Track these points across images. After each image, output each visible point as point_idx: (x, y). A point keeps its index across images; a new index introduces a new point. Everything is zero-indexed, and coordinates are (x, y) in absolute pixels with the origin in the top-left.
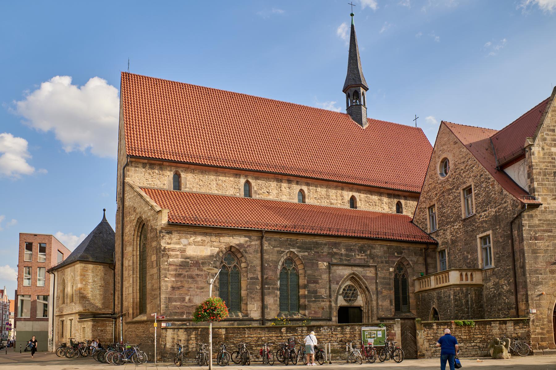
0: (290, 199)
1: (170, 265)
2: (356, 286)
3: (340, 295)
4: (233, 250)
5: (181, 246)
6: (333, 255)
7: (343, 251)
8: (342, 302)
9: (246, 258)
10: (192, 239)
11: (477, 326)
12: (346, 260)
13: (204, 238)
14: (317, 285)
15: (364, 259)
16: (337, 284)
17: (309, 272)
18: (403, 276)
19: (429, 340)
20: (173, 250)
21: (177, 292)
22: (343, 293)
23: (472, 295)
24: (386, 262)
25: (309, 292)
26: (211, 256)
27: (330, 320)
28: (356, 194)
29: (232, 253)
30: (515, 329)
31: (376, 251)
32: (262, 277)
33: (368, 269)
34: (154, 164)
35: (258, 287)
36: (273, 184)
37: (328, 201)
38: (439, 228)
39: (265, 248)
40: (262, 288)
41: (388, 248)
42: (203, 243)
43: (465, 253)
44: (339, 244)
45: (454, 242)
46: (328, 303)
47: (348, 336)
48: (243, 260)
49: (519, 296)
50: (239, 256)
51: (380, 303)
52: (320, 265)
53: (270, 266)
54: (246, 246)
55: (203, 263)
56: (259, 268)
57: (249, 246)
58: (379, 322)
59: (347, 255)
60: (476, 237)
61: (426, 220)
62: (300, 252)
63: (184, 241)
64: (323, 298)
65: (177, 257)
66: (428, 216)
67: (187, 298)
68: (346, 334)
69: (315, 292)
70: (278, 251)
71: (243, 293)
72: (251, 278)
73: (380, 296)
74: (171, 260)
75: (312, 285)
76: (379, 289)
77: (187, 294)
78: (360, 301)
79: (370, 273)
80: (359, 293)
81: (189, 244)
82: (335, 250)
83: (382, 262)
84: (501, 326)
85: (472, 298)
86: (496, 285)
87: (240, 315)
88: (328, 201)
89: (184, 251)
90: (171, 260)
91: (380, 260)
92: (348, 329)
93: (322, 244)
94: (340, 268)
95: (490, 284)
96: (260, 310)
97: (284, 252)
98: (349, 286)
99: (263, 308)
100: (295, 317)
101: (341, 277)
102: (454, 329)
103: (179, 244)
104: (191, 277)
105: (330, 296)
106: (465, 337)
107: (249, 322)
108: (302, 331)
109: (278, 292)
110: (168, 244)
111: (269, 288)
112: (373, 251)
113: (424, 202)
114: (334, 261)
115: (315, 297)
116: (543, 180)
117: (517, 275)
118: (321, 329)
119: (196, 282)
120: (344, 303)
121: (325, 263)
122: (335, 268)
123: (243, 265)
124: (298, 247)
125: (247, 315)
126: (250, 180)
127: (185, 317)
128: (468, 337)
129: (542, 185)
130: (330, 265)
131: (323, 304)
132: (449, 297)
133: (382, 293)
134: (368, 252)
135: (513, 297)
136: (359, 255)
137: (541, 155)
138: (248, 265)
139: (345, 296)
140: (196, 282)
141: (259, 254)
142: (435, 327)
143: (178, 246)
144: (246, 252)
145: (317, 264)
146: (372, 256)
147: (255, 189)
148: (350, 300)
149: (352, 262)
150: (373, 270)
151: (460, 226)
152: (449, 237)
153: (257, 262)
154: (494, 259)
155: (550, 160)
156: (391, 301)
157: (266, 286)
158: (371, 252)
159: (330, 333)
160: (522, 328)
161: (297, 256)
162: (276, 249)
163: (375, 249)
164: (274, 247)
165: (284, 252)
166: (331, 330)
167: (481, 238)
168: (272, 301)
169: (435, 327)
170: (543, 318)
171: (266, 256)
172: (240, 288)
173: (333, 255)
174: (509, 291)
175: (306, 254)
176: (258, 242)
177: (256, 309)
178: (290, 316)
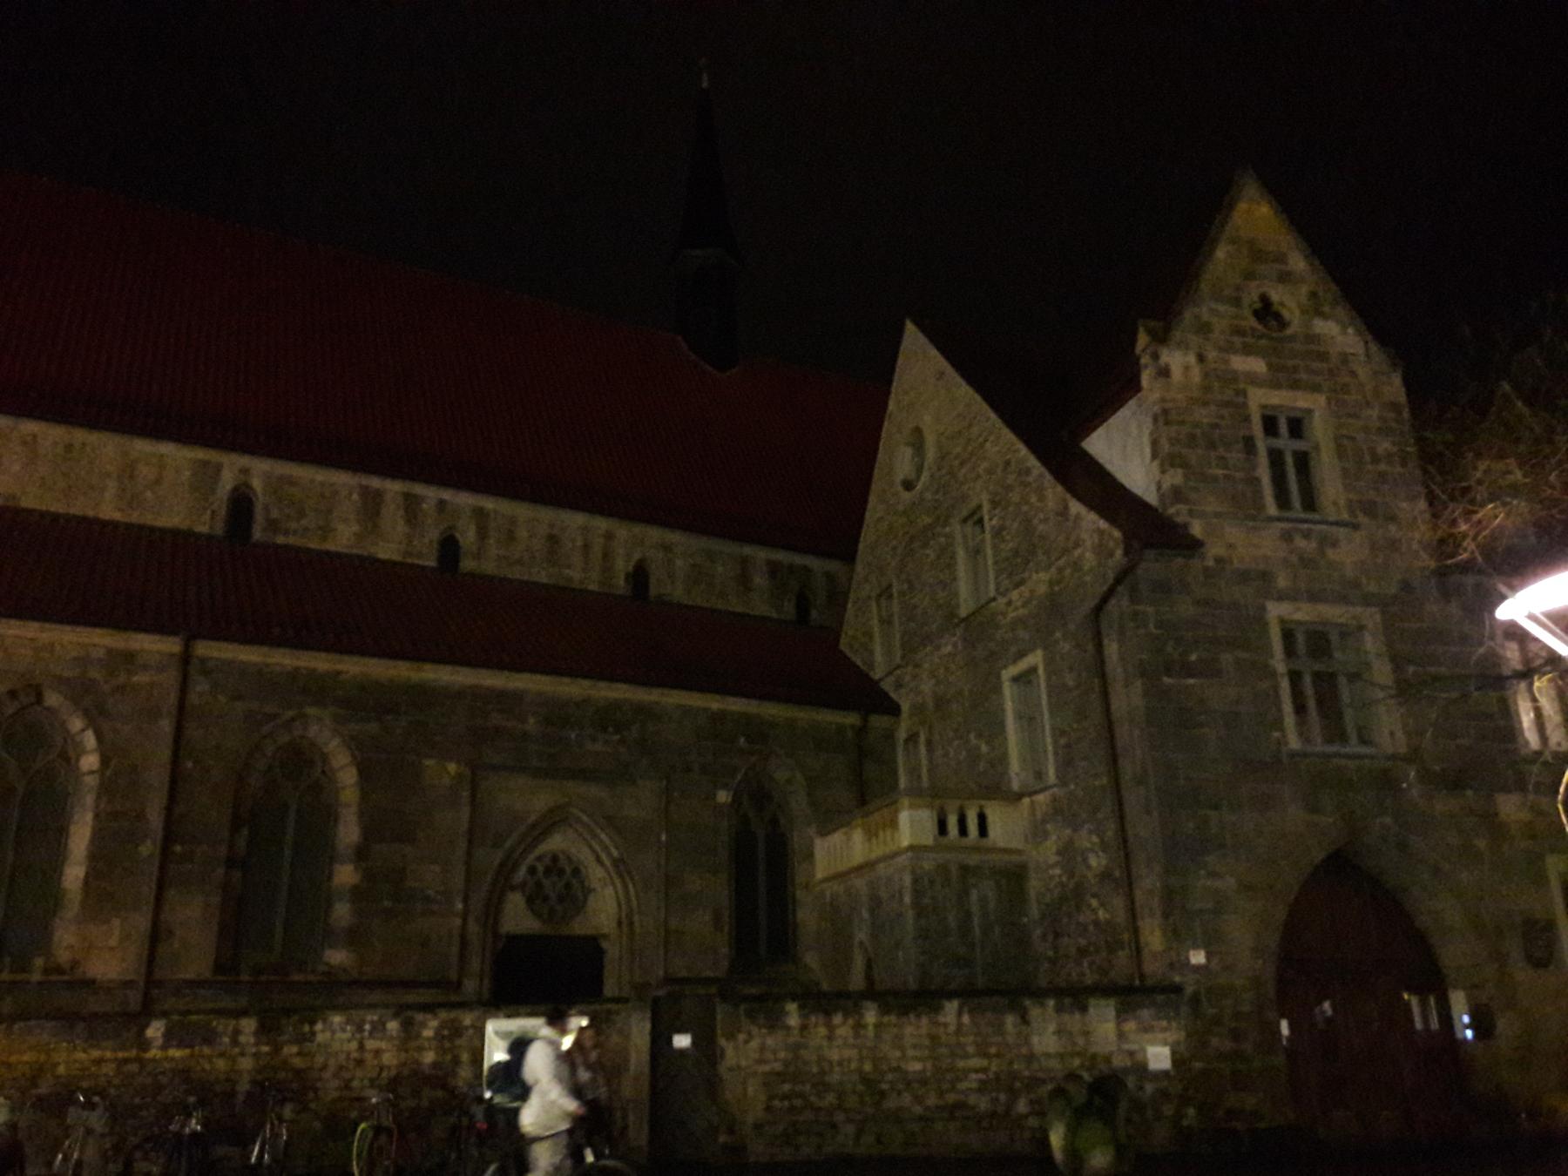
11: (966, 1019)
18: (774, 822)
23: (983, 894)
30: (1121, 1035)
38: (903, 657)
39: (193, 698)
43: (972, 736)
45: (941, 702)
49: (1138, 894)
54: (106, 688)
57: (121, 689)
60: (999, 677)
61: (871, 637)
64: (427, 899)
66: (875, 622)
68: (420, 1049)
71: (74, 874)
84: (1066, 1017)
85: (983, 900)
86: (1067, 852)
92: (430, 1028)
95: (1048, 851)
97: (275, 716)
98: (555, 859)
99: (157, 935)
102: (871, 1032)
106: (917, 1066)
113: (866, 580)
117: (1127, 809)
118: (319, 1026)
121: (452, 767)
128: (929, 1065)
132: (901, 900)
135: (1119, 903)
138: (105, 761)
142: (793, 1020)
147: (275, 514)
151: (955, 645)
152: (927, 687)
154: (1056, 754)
157: (178, 848)
159: (354, 1045)
166: (360, 1029)
167: (1015, 679)
169: (793, 1020)
174: (1105, 876)
177: (113, 942)
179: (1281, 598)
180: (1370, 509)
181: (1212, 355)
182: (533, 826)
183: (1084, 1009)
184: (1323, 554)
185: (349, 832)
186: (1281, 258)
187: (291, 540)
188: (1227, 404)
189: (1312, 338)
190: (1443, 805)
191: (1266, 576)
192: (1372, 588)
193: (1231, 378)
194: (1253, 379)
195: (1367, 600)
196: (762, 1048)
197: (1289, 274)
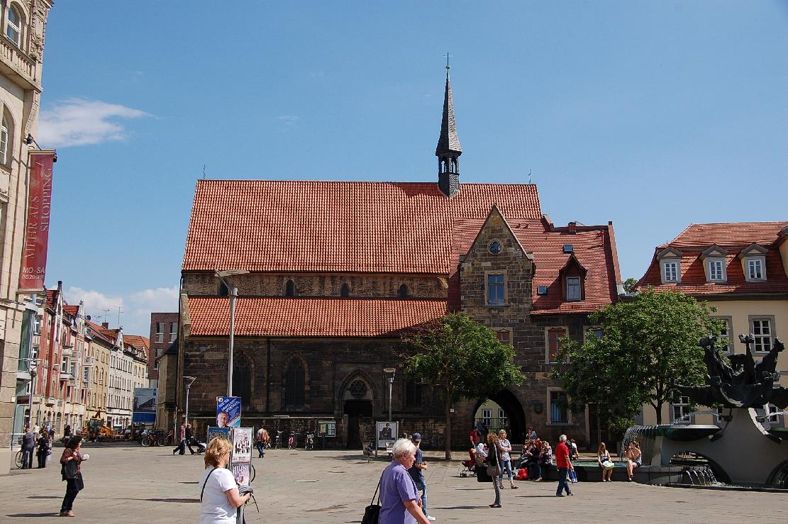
2: (365, 382)
8: (348, 396)
19: (367, 434)
20: (195, 356)
22: (351, 388)
25: (311, 388)
28: (407, 282)
30: (435, 427)
32: (268, 376)
34: (206, 275)
35: (265, 384)
40: (268, 385)
42: (218, 350)
48: (252, 361)
56: (265, 369)
63: (203, 349)
65: (197, 362)
67: (204, 394)
71: (252, 389)
72: (258, 377)
74: (192, 364)
77: (204, 392)
78: (369, 395)
80: (369, 388)
81: (207, 351)
90: (192, 364)
94: (345, 365)
96: (265, 404)
98: (358, 382)
99: (268, 401)
104: (208, 377)
111: (273, 385)
116: (470, 293)
123: (253, 366)
124: (303, 349)
134: (376, 349)
137: (471, 270)
139: (353, 390)
141: (266, 357)
148: (358, 395)
153: (265, 363)
156: (399, 396)
162: (281, 351)
168: (275, 396)
176: (265, 347)
180: (513, 300)
181: (476, 262)
182: (350, 375)
183: (428, 421)
185: (307, 379)
186: (501, 230)
189: (506, 254)
194: (487, 268)
196: (367, 427)
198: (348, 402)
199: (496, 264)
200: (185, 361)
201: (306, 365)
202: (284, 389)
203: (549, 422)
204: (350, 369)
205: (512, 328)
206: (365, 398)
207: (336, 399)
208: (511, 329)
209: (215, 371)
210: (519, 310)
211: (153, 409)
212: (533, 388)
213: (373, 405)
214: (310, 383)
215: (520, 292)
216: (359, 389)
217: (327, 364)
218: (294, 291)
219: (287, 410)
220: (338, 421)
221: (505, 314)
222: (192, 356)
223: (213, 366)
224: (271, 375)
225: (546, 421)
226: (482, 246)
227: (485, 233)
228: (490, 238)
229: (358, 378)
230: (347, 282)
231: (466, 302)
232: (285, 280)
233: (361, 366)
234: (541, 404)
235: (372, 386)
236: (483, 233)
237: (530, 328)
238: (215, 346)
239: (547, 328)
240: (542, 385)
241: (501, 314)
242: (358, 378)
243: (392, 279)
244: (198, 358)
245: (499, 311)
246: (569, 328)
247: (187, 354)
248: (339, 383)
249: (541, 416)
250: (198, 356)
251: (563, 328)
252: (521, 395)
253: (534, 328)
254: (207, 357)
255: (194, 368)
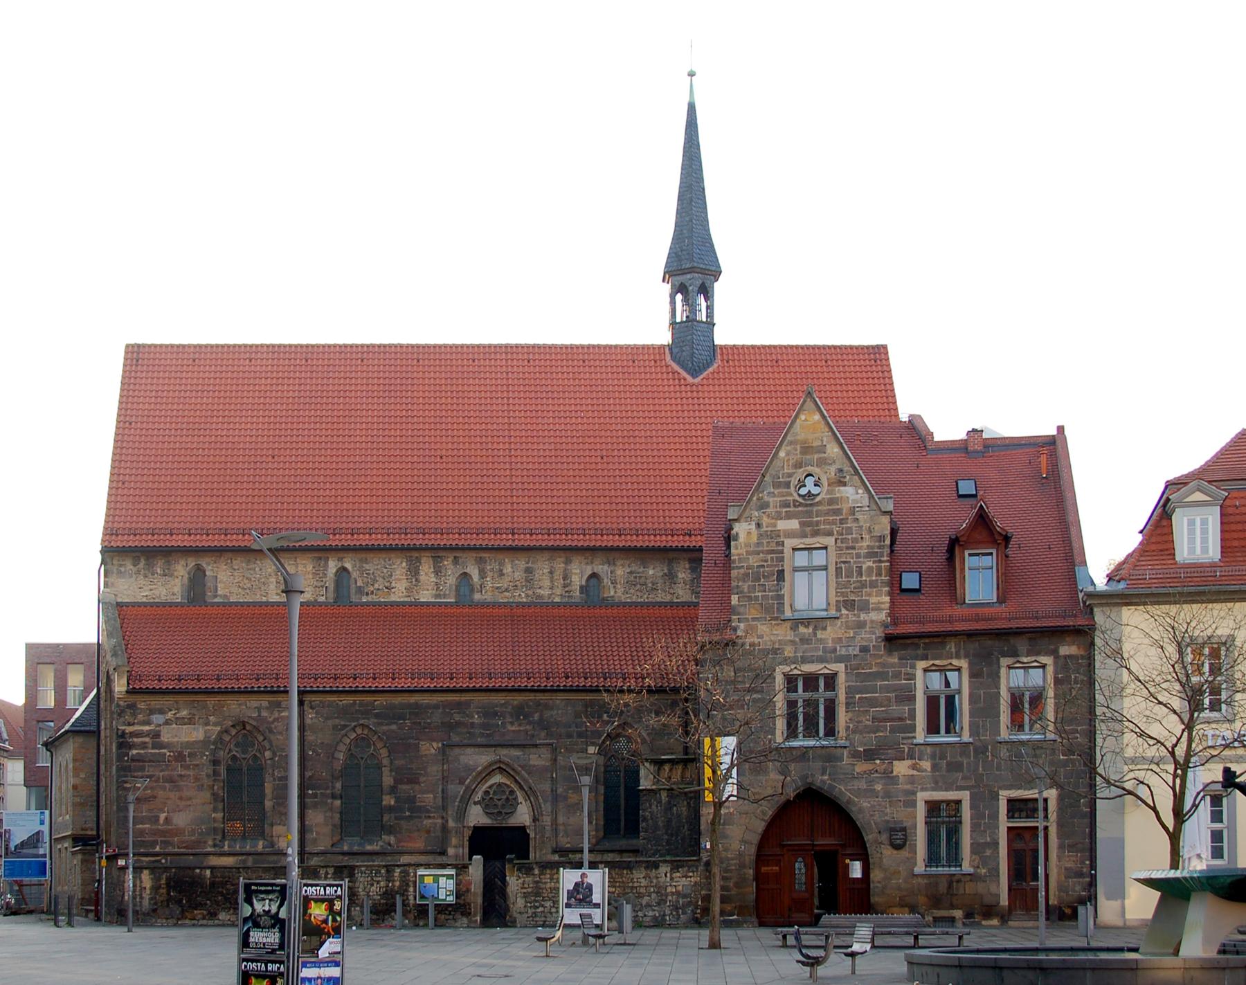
0: (437, 596)
1: (133, 760)
3: (475, 803)
4: (248, 727)
5: (152, 727)
6: (450, 727)
7: (476, 719)
8: (477, 816)
9: (270, 742)
10: (170, 715)
12: (482, 735)
13: (194, 711)
14: (417, 787)
15: (526, 731)
16: (462, 782)
17: (399, 762)
19: (525, 896)
21: (145, 807)
24: (580, 735)
25: (398, 800)
26: (205, 743)
27: (443, 853)
28: (602, 569)
29: (245, 731)
30: (672, 879)
31: (554, 712)
33: (533, 750)
36: (399, 567)
37: (530, 592)
39: (308, 721)
41: (586, 706)
42: (190, 721)
44: (468, 704)
46: (440, 821)
47: (397, 884)
48: (266, 744)
50: (261, 738)
51: (561, 820)
52: (423, 748)
53: (318, 754)
55: (190, 755)
57: (276, 720)
58: (556, 857)
59: (484, 726)
62: (381, 724)
63: (158, 719)
64: (428, 811)
67: (163, 816)
69: (412, 800)
70: (335, 727)
73: (561, 805)
74: (135, 752)
75: (404, 787)
76: (560, 790)
78: (522, 815)
79: (538, 759)
80: (520, 799)
81: (167, 723)
82: (457, 717)
83: (569, 736)
87: (260, 845)
88: (530, 592)
89: (157, 735)
90: (135, 752)
91: (563, 731)
93: (428, 706)
94: (469, 750)
97: (346, 726)
98: (500, 785)
100: (369, 848)
101: (469, 769)
103: (148, 723)
104: (171, 780)
105: (444, 808)
107: (275, 858)
108: (327, 873)
109: (338, 803)
110: (129, 724)
111: (315, 796)
112: (547, 714)
114: (455, 739)
115: (411, 810)
119: (179, 789)
120: (485, 821)
121: (435, 745)
122: (457, 751)
123: (268, 754)
124: (377, 716)
125: (272, 845)
126: (348, 565)
127: (158, 849)
129: (750, 598)
130: (448, 747)
131: (427, 822)
133: (566, 798)
134: (536, 716)
136: (512, 723)
137: (754, 538)
138: (274, 754)
139: (488, 804)
140: (179, 789)
142: (536, 872)
143: (147, 728)
144: (271, 731)
145: (417, 746)
146: (544, 725)
149: (497, 739)
150: (546, 754)
155: (773, 546)
158: (541, 716)
160: (686, 877)
161: (376, 732)
162: (330, 723)
163: (552, 709)
164: (327, 719)
165: (346, 726)
169: (536, 872)
170: (728, 859)
171: (310, 737)
172: (263, 796)
173: (450, 727)
175: (394, 727)
178: (359, 845)
179: (785, 661)
180: (849, 605)
181: (765, 521)
182: (480, 773)
183: (657, 867)
184: (815, 634)
185: (388, 780)
187: (370, 598)
188: (772, 552)
190: (861, 767)
191: (775, 651)
192: (843, 652)
193: (774, 535)
195: (839, 660)
197: (825, 459)
198: (478, 831)
199: (809, 524)
200: (121, 746)
201: (384, 752)
202: (338, 803)
203: (920, 868)
204: (482, 759)
205: (843, 665)
206: (514, 821)
207: (451, 824)
208: (840, 668)
209: (188, 767)
210: (861, 625)
211: (41, 851)
212: (887, 795)
213: (532, 835)
214: (393, 790)
215: (863, 585)
216: (500, 802)
217: (430, 748)
218: (353, 591)
219: (346, 848)
220: (462, 868)
221: (829, 635)
222: (133, 734)
223: (180, 757)
224: (308, 774)
225: (916, 864)
226: (776, 485)
227: (788, 454)
228: (798, 465)
229: (498, 779)
230: (468, 571)
231: (742, 610)
232: (332, 566)
233: (504, 752)
234: (904, 829)
235: (530, 793)
236: (782, 454)
237: (884, 665)
238: (184, 713)
239: (921, 665)
240: (908, 787)
241: (820, 634)
242: (498, 779)
243: (568, 562)
244: (147, 739)
245: (815, 628)
246: (970, 664)
247: (123, 731)
248: (457, 790)
249: (904, 853)
250: (148, 734)
251: (955, 662)
252: (861, 810)
253: (893, 665)
254: (166, 737)
255: (138, 761)
